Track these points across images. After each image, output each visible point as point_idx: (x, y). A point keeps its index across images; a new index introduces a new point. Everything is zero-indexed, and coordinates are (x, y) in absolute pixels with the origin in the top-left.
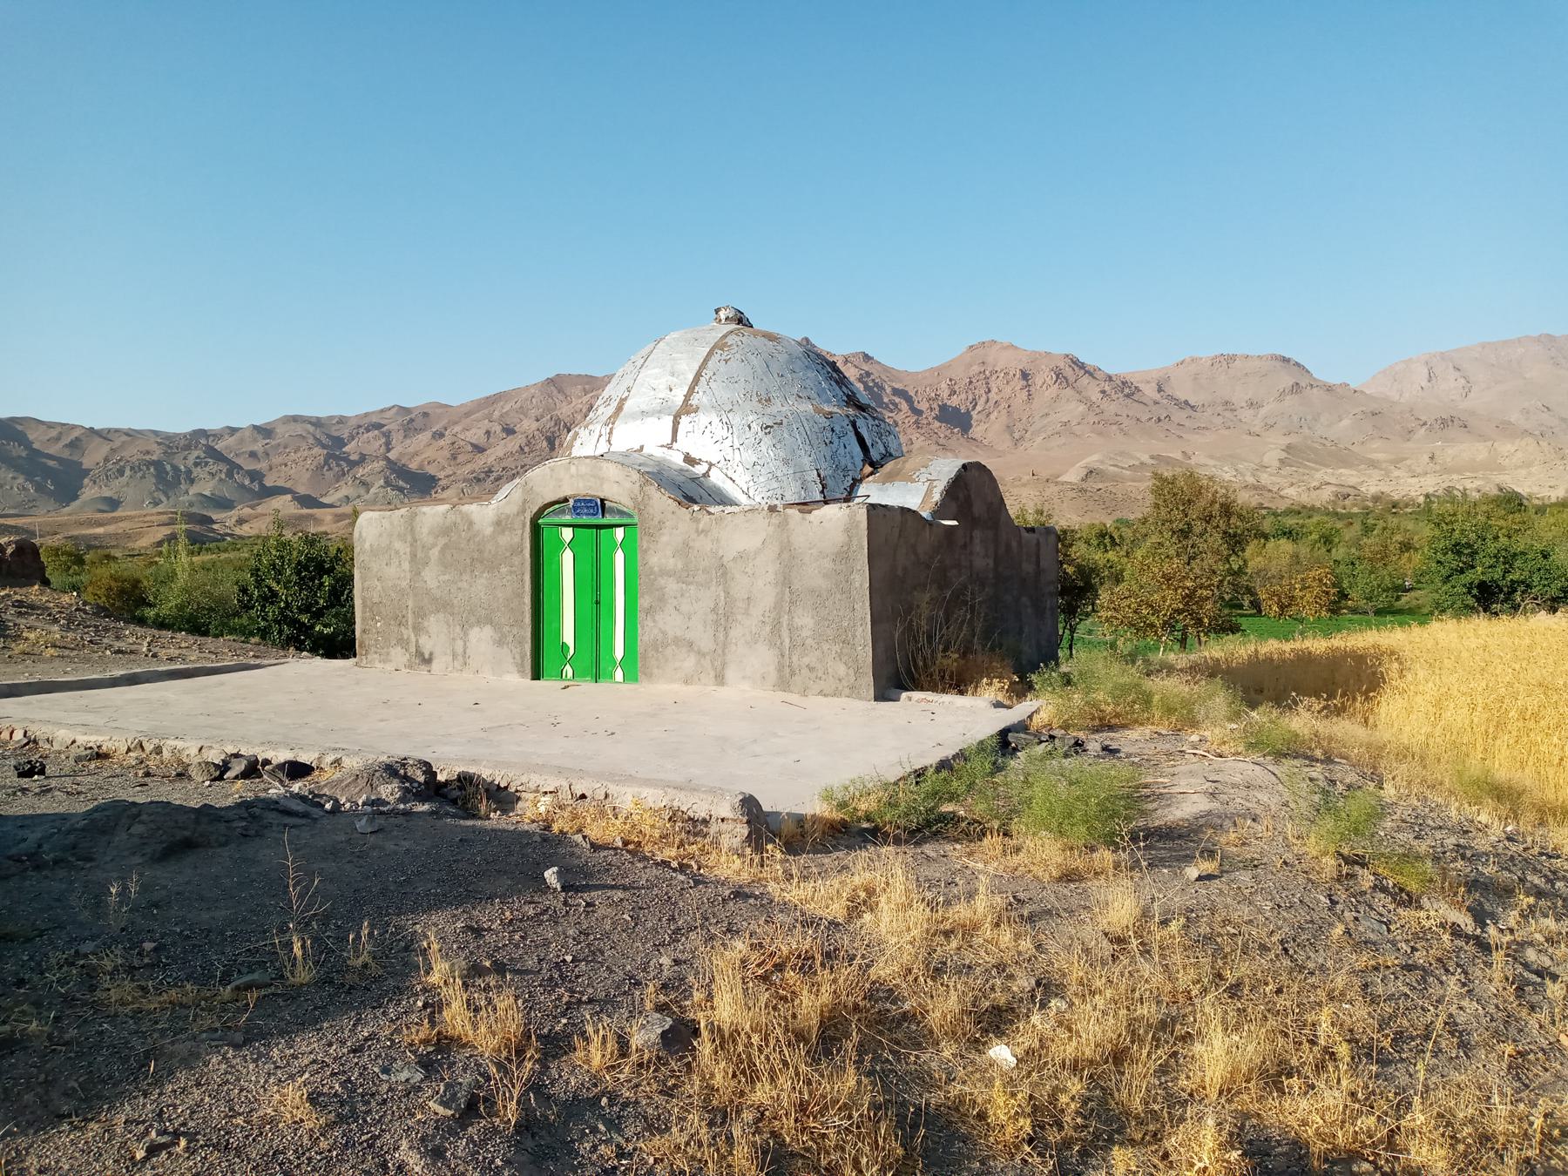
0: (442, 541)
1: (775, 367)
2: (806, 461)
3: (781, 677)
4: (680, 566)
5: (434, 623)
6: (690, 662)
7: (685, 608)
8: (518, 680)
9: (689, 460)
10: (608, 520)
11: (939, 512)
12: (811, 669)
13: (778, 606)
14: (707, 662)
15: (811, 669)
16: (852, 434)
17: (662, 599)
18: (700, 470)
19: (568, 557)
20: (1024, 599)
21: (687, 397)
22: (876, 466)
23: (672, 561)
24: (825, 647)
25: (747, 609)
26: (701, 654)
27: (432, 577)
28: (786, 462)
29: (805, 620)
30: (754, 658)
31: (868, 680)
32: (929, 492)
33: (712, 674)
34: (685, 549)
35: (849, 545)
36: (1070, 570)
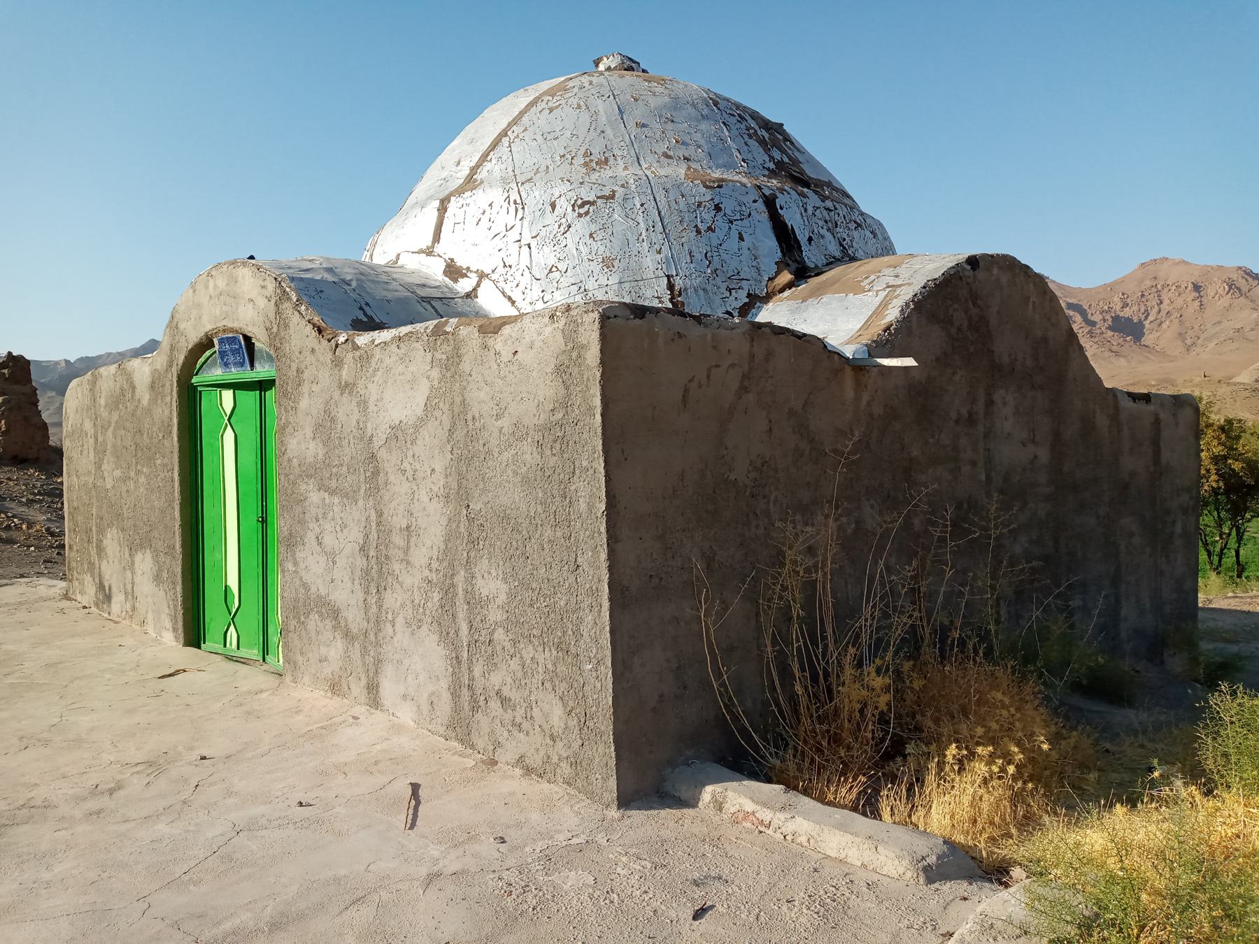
0: (115, 417)
1: (637, 113)
2: (650, 262)
3: (457, 709)
4: (320, 456)
5: (112, 541)
6: (334, 652)
7: (328, 540)
8: (166, 640)
9: (453, 271)
10: (262, 371)
11: (890, 342)
12: (505, 701)
13: (447, 552)
14: (356, 654)
15: (505, 701)
16: (761, 215)
17: (302, 522)
18: (464, 285)
19: (229, 436)
20: (1128, 522)
21: (474, 170)
22: (802, 274)
23: (312, 445)
24: (528, 652)
25: (406, 551)
26: (348, 635)
28: (608, 263)
30: (418, 665)
31: (604, 753)
32: (884, 305)
33: (364, 682)
34: (326, 427)
35: (565, 404)
36: (1237, 466)
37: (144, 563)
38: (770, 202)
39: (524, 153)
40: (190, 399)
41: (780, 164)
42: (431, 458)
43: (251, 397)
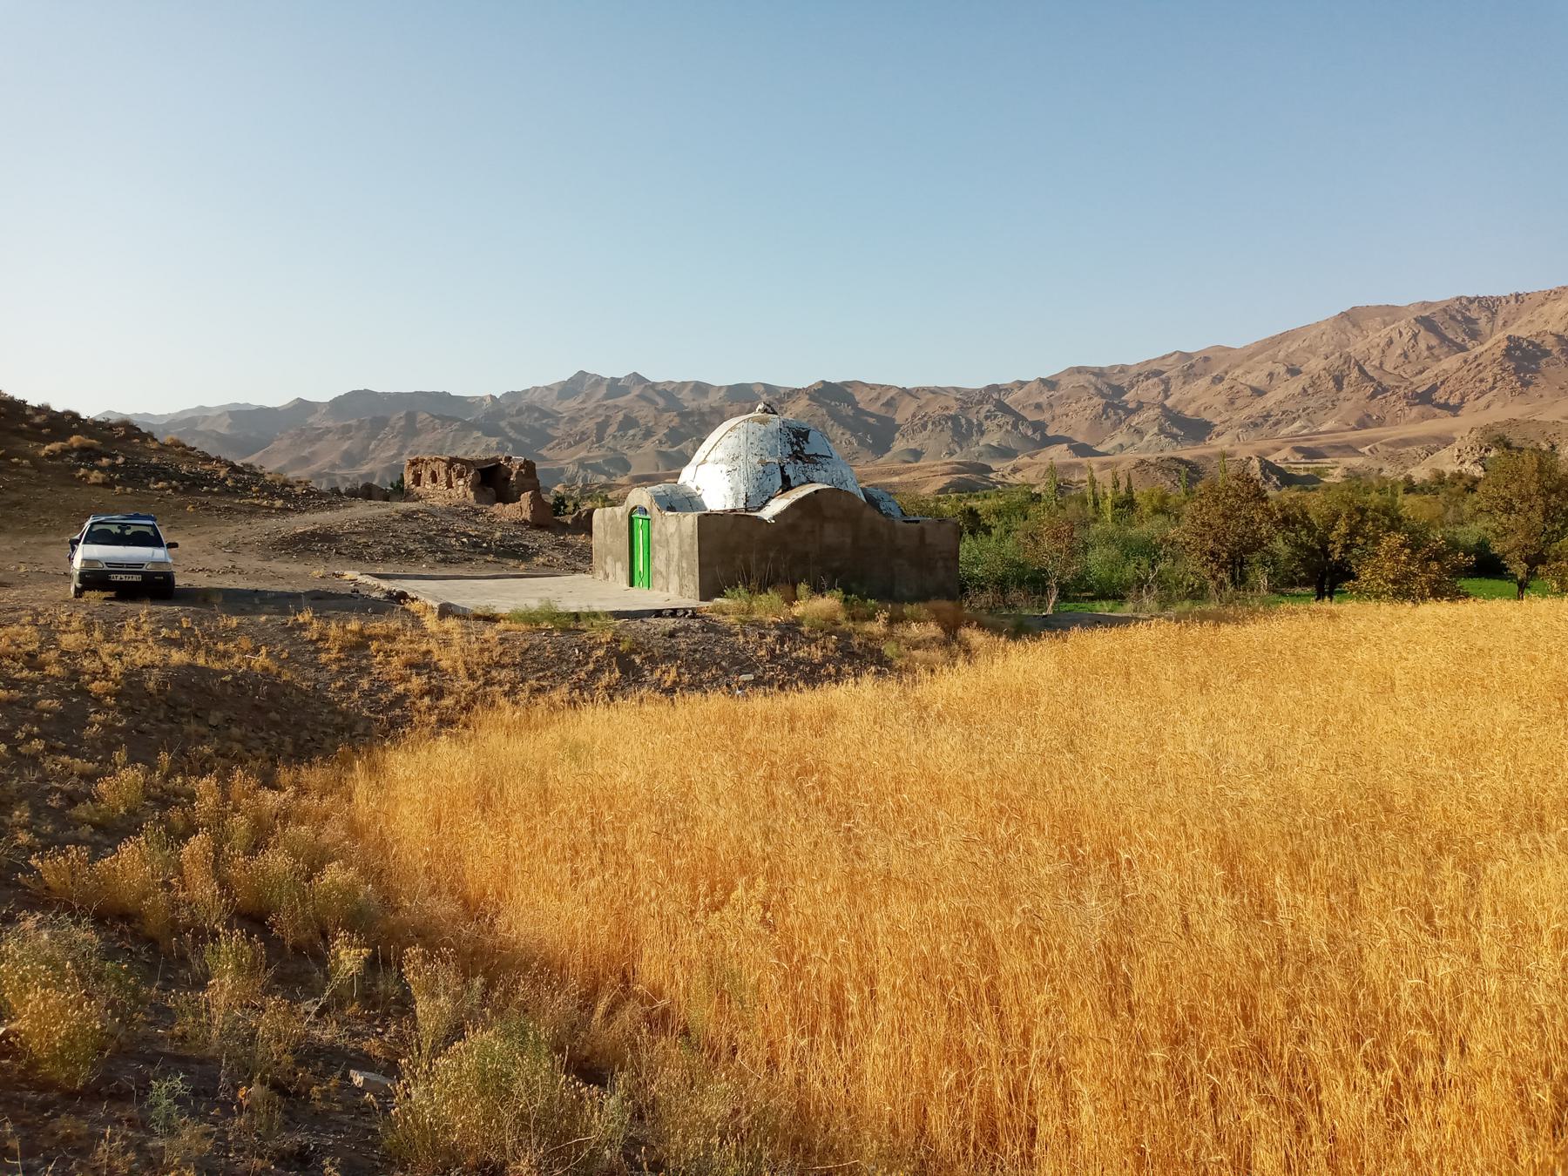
2: (742, 488)
5: (609, 559)
8: (626, 586)
30: (674, 581)
34: (660, 532)
37: (619, 565)
38: (782, 469)
39: (719, 454)
40: (631, 521)
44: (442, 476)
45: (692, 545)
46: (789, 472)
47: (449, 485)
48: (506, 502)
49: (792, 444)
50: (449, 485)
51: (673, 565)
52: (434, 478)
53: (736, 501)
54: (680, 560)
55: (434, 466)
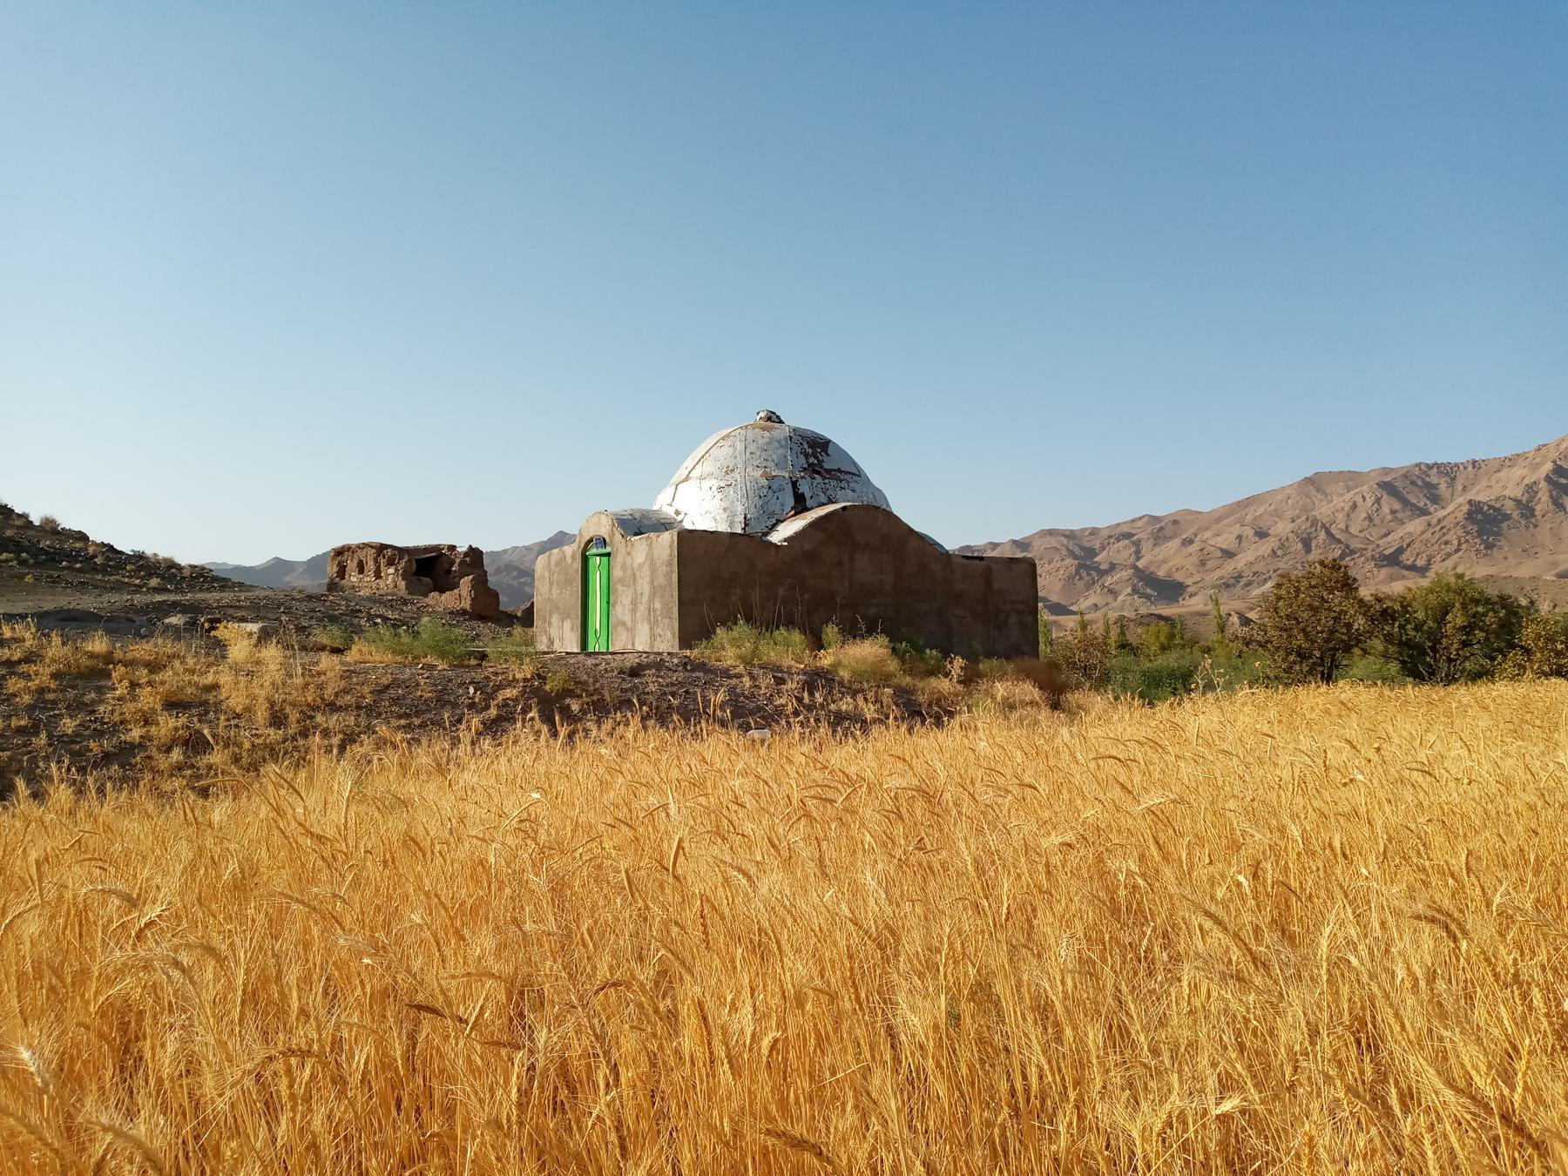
1: (751, 448)
2: (740, 509)
5: (555, 619)
9: (678, 513)
10: (608, 550)
16: (789, 488)
18: (679, 518)
27: (555, 591)
29: (658, 605)
37: (567, 624)
38: (794, 484)
39: (708, 467)
40: (585, 560)
41: (810, 465)
42: (646, 572)
43: (605, 559)
44: (371, 565)
45: (669, 575)
46: (804, 488)
47: (378, 575)
48: (442, 591)
49: (807, 456)
50: (378, 575)
51: (642, 608)
52: (361, 568)
53: (731, 525)
54: (651, 600)
55: (361, 554)
